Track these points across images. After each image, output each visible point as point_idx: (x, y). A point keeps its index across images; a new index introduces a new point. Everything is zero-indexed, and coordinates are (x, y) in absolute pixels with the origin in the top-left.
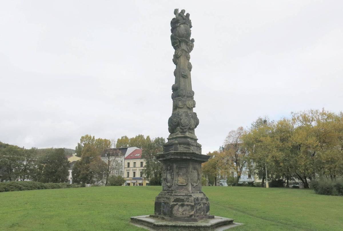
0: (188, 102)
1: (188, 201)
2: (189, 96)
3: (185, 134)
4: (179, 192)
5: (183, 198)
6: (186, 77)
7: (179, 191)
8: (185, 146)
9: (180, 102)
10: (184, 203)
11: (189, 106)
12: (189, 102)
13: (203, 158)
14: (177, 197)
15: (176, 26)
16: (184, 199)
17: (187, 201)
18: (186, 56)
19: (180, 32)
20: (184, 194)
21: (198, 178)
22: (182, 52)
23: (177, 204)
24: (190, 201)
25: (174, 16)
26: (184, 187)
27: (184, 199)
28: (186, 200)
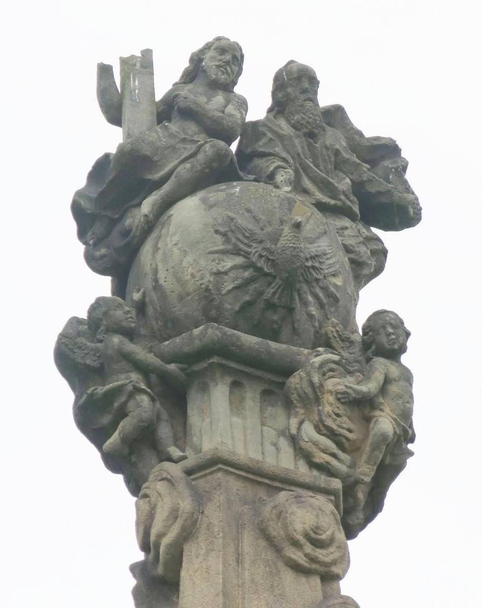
15: (126, 233)
18: (264, 533)
19: (162, 275)
22: (200, 499)
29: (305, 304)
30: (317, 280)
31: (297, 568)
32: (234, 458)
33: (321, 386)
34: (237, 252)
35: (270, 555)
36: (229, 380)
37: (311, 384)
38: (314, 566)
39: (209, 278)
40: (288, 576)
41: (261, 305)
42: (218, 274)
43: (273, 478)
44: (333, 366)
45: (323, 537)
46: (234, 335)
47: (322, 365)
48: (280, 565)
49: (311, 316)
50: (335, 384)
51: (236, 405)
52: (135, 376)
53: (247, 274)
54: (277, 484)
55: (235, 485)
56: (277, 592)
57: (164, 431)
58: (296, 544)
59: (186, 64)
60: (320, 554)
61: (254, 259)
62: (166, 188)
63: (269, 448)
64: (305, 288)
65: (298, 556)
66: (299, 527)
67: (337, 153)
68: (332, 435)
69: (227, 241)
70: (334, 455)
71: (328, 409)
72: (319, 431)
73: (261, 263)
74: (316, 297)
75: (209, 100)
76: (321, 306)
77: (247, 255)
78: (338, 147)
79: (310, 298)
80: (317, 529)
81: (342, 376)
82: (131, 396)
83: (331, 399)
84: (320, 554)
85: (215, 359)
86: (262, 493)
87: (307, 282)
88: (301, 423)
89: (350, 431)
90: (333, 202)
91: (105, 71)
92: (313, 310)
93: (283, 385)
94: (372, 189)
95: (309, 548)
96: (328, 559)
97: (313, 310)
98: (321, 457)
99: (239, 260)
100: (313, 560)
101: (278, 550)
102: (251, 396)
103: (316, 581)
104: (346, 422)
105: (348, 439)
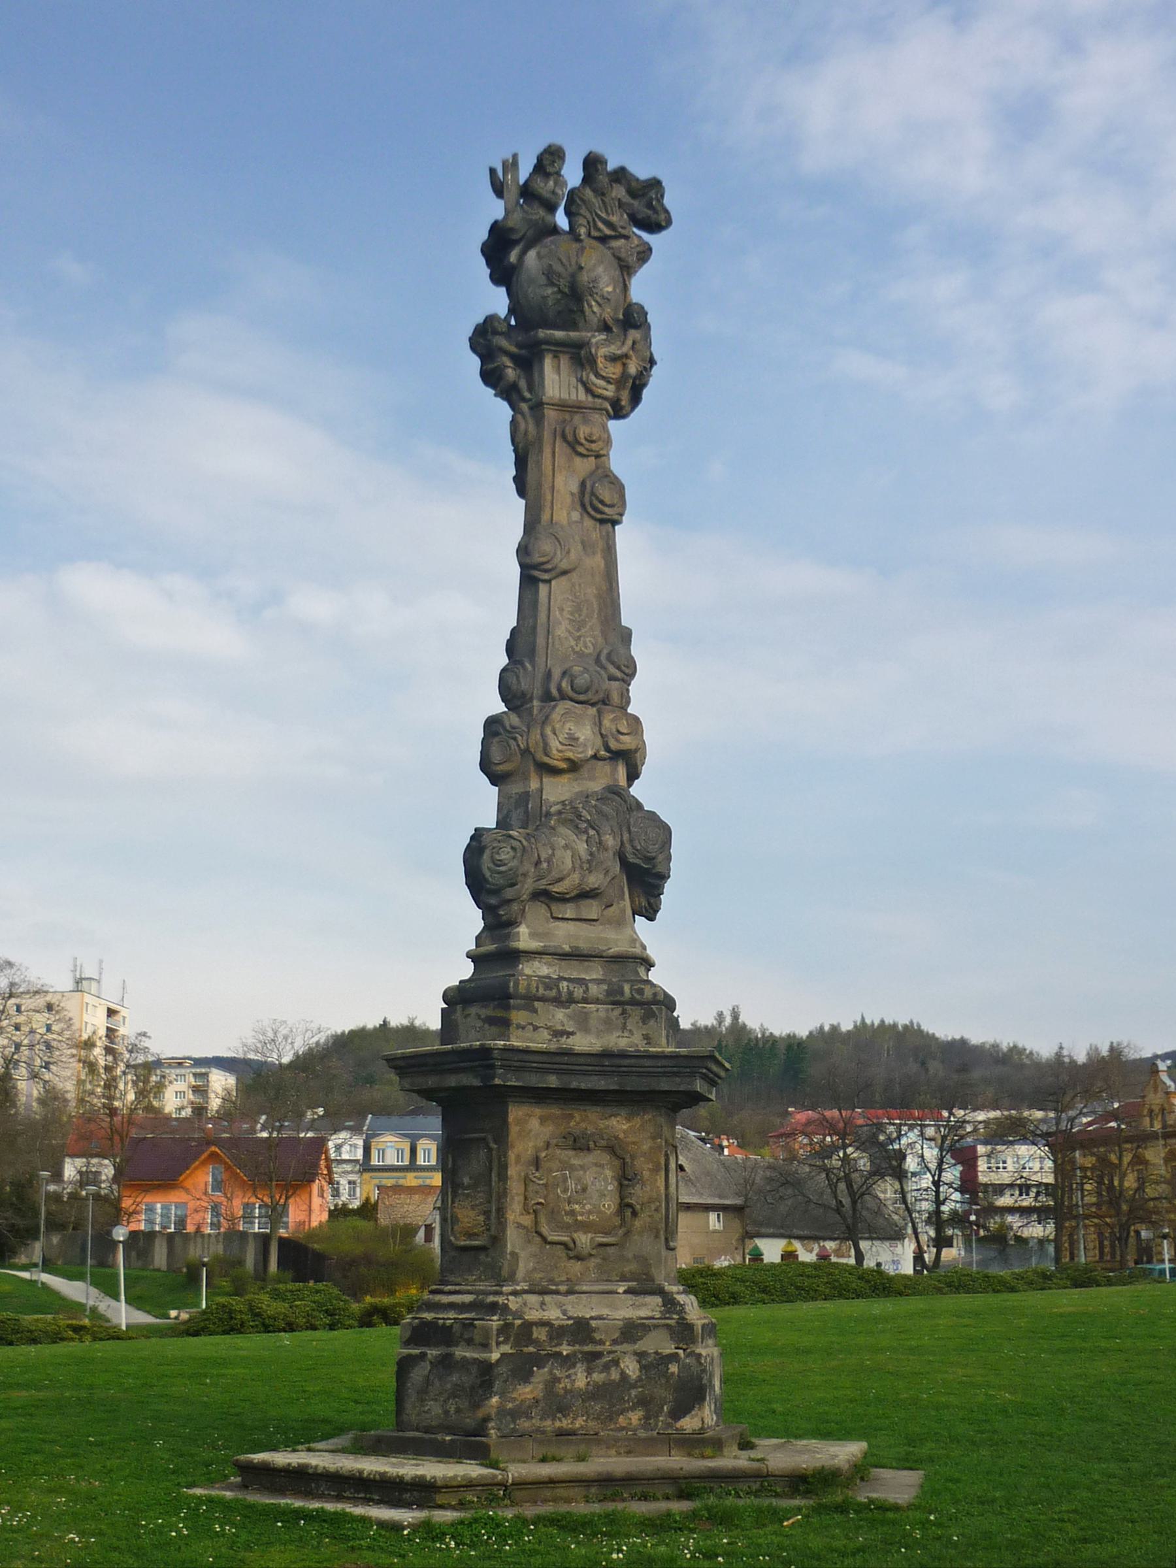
1: (470, 1342)
3: (508, 937)
4: (457, 1288)
5: (449, 1322)
6: (546, 576)
7: (458, 1280)
9: (496, 739)
13: (538, 1070)
14: (428, 1316)
16: (451, 1326)
17: (466, 1337)
18: (564, 437)
20: (468, 1298)
21: (622, 1198)
23: (423, 1356)
25: (496, 209)
26: (482, 1257)
27: (454, 1330)
28: (462, 1334)
29: (590, 306)
33: (596, 354)
35: (569, 450)
44: (603, 342)
45: (594, 438)
47: (596, 343)
49: (594, 312)
50: (603, 351)
53: (559, 296)
59: (535, 161)
60: (593, 446)
64: (589, 298)
69: (548, 278)
74: (597, 302)
75: (546, 185)
76: (599, 305)
77: (558, 286)
78: (619, 197)
79: (593, 303)
80: (591, 435)
81: (608, 346)
84: (593, 446)
86: (567, 417)
87: (591, 295)
89: (614, 374)
90: (613, 233)
92: (596, 309)
94: (640, 216)
97: (596, 309)
99: (556, 289)
105: (613, 379)
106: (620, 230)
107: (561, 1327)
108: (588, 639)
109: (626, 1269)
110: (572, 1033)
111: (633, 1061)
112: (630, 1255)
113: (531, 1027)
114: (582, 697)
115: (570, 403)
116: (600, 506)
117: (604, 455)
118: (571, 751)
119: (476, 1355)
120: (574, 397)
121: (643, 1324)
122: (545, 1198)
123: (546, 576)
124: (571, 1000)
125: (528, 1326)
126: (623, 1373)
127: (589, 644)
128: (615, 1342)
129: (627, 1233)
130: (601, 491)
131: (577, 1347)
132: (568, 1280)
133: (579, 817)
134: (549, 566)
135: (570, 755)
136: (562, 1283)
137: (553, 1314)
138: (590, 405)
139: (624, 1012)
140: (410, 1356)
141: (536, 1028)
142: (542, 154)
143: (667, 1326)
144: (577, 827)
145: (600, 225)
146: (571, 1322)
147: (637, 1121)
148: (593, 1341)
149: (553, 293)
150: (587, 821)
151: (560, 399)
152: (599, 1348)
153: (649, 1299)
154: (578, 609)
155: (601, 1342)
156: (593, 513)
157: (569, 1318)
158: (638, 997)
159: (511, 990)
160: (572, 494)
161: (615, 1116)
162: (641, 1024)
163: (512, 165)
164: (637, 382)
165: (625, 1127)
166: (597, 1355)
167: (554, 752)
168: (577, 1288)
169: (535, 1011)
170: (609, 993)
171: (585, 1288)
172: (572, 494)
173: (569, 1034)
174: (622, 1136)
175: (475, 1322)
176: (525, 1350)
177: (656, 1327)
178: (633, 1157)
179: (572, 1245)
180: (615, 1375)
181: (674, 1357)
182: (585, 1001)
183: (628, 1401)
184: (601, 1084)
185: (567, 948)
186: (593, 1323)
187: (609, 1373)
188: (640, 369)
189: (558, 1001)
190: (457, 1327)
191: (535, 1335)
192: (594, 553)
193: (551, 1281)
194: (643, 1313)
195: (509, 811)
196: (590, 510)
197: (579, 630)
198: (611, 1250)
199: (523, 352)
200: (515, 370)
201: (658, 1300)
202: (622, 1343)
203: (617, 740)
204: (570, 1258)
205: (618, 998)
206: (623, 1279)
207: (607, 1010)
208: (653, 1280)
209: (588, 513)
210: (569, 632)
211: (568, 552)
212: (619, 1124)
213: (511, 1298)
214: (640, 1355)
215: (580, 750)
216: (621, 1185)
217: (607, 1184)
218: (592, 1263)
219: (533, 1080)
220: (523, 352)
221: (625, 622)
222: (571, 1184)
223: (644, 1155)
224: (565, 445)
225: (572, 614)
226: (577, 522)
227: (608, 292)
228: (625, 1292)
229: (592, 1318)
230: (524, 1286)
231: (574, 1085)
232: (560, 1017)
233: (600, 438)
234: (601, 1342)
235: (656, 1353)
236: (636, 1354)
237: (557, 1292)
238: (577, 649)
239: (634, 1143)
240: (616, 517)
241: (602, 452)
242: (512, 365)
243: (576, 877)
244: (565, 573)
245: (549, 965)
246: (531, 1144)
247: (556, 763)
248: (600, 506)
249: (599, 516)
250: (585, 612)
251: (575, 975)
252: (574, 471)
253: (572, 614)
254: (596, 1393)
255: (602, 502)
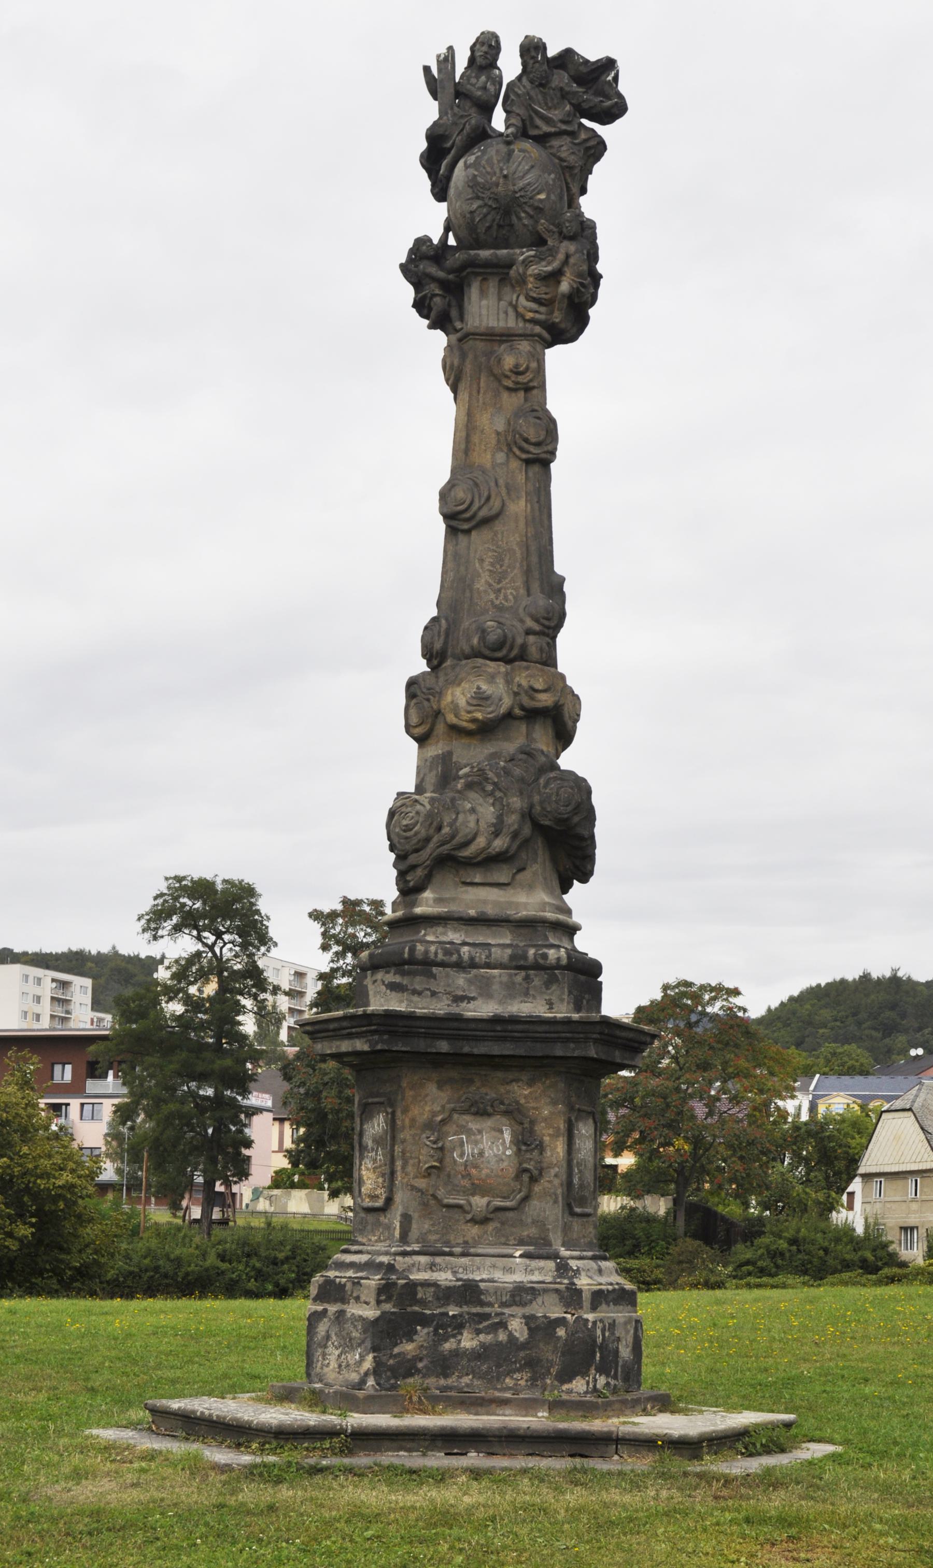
0: (450, 692)
2: (472, 648)
6: (466, 526)
8: (391, 977)
10: (345, 1307)
11: (456, 716)
12: (458, 691)
16: (345, 1285)
18: (491, 373)
20: (364, 1258)
21: (520, 1164)
23: (325, 1311)
24: (363, 1298)
29: (520, 219)
30: (525, 203)
31: (509, 389)
32: (478, 331)
33: (525, 273)
34: (478, 198)
36: (480, 278)
37: (519, 274)
38: (518, 386)
39: (468, 215)
40: (505, 395)
41: (495, 227)
42: (471, 212)
43: (501, 335)
44: (532, 259)
46: (475, 254)
47: (524, 261)
48: (501, 389)
49: (524, 225)
51: (483, 293)
52: (433, 286)
53: (485, 210)
54: (504, 338)
55: (480, 345)
56: (498, 406)
57: (454, 313)
58: (507, 377)
60: (521, 379)
61: (486, 201)
62: (453, 152)
63: (502, 316)
64: (518, 209)
65: (509, 383)
66: (507, 367)
67: (561, 89)
68: (534, 300)
70: (536, 312)
71: (530, 286)
72: (528, 300)
73: (490, 203)
74: (525, 212)
76: (532, 217)
77: (483, 199)
78: (561, 85)
79: (523, 215)
80: (517, 366)
82: (431, 298)
83: (531, 279)
84: (521, 379)
85: (469, 270)
87: (519, 206)
88: (518, 297)
89: (546, 294)
90: (553, 130)
91: (427, 70)
92: (526, 222)
93: (508, 273)
94: (585, 106)
95: (513, 378)
96: (525, 381)
98: (529, 315)
99: (480, 202)
100: (518, 383)
101: (499, 381)
102: (492, 286)
103: (521, 394)
104: (544, 289)
106: (559, 125)
107: (448, 1288)
108: (509, 591)
109: (525, 1233)
110: (473, 999)
111: (526, 1027)
112: (529, 1220)
113: (428, 993)
114: (499, 654)
115: (497, 331)
116: (525, 445)
117: (534, 388)
118: (480, 711)
119: (360, 1313)
120: (502, 324)
121: (533, 1288)
122: (441, 1161)
123: (466, 526)
124: (473, 965)
125: (412, 1286)
126: (511, 1334)
127: (510, 597)
128: (503, 1305)
129: (526, 1199)
130: (524, 428)
131: (465, 1309)
132: (466, 1242)
133: (487, 779)
134: (467, 515)
135: (479, 716)
136: (458, 1245)
137: (444, 1277)
138: (520, 332)
139: (527, 978)
140: (316, 1312)
141: (434, 994)
142: (474, 45)
143: (557, 1291)
144: (483, 790)
145: (538, 122)
146: (460, 1283)
147: (538, 1088)
148: (482, 1304)
149: (480, 207)
150: (495, 784)
151: (488, 328)
152: (487, 1310)
153: (542, 1263)
154: (499, 560)
155: (490, 1305)
156: (518, 452)
157: (458, 1280)
158: (541, 961)
159: (406, 956)
160: (498, 433)
161: (516, 1080)
162: (544, 989)
163: (447, 60)
164: (576, 300)
165: (526, 1092)
166: (487, 1316)
167: (463, 713)
168: (472, 1250)
169: (434, 977)
170: (512, 957)
171: (480, 1251)
172: (498, 433)
173: (470, 999)
174: (522, 1101)
175: (362, 1281)
176: (409, 1309)
177: (545, 1291)
178: (532, 1122)
179: (467, 1208)
180: (502, 1336)
181: (561, 1322)
182: (488, 966)
183: (515, 1362)
184: (496, 1049)
185: (472, 912)
186: (482, 1285)
187: (496, 1335)
188: (575, 286)
189: (459, 966)
190: (349, 1286)
191: (419, 1296)
192: (518, 498)
193: (447, 1243)
194: (536, 1277)
195: (425, 775)
196: (516, 450)
197: (499, 582)
198: (510, 1214)
199: (451, 277)
200: (445, 297)
201: (551, 1264)
202: (510, 1306)
203: (532, 698)
204: (468, 1222)
205: (522, 963)
206: (521, 1242)
207: (510, 975)
208: (551, 1245)
209: (514, 454)
210: (490, 585)
211: (488, 498)
212: (521, 1092)
213: (398, 1258)
214: (529, 1319)
215: (490, 709)
216: (519, 1150)
217: (505, 1148)
218: (491, 1227)
219: (421, 1045)
220: (451, 277)
221: (559, 568)
222: (468, 1149)
223: (545, 1120)
224: (492, 378)
225: (492, 564)
226: (501, 464)
227: (541, 201)
228: (521, 1256)
229: (482, 1281)
230: (416, 1247)
231: (466, 1049)
232: (460, 981)
233: (527, 369)
234: (490, 1305)
235: (545, 1317)
236: (524, 1317)
237: (451, 1254)
238: (497, 602)
239: (534, 1108)
240: (544, 456)
241: (531, 384)
242: (440, 293)
243: (481, 841)
244: (487, 521)
245: (455, 930)
246: (427, 1108)
247: (465, 724)
248: (525, 445)
249: (524, 456)
250: (506, 561)
251: (481, 939)
252: (501, 408)
253: (492, 564)
254: (481, 1354)
255: (526, 440)
